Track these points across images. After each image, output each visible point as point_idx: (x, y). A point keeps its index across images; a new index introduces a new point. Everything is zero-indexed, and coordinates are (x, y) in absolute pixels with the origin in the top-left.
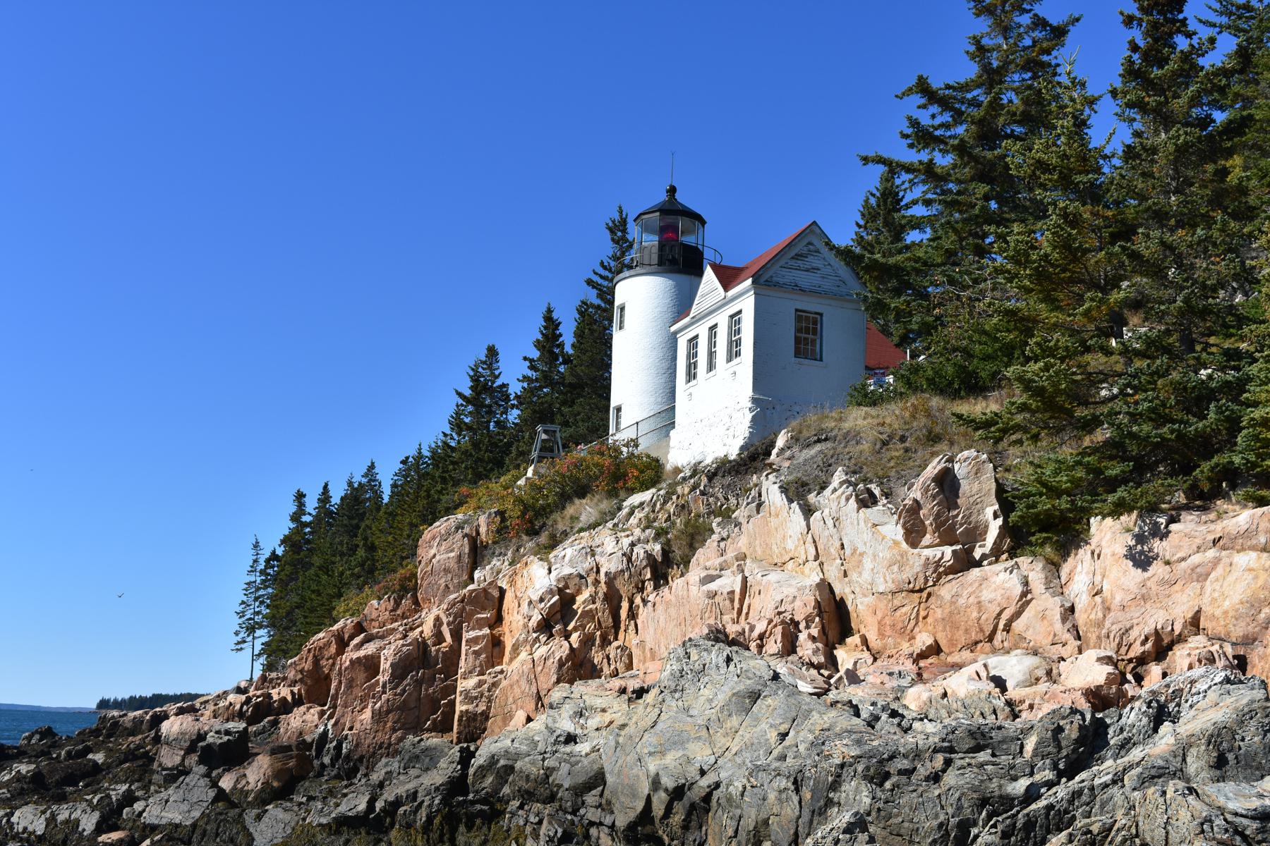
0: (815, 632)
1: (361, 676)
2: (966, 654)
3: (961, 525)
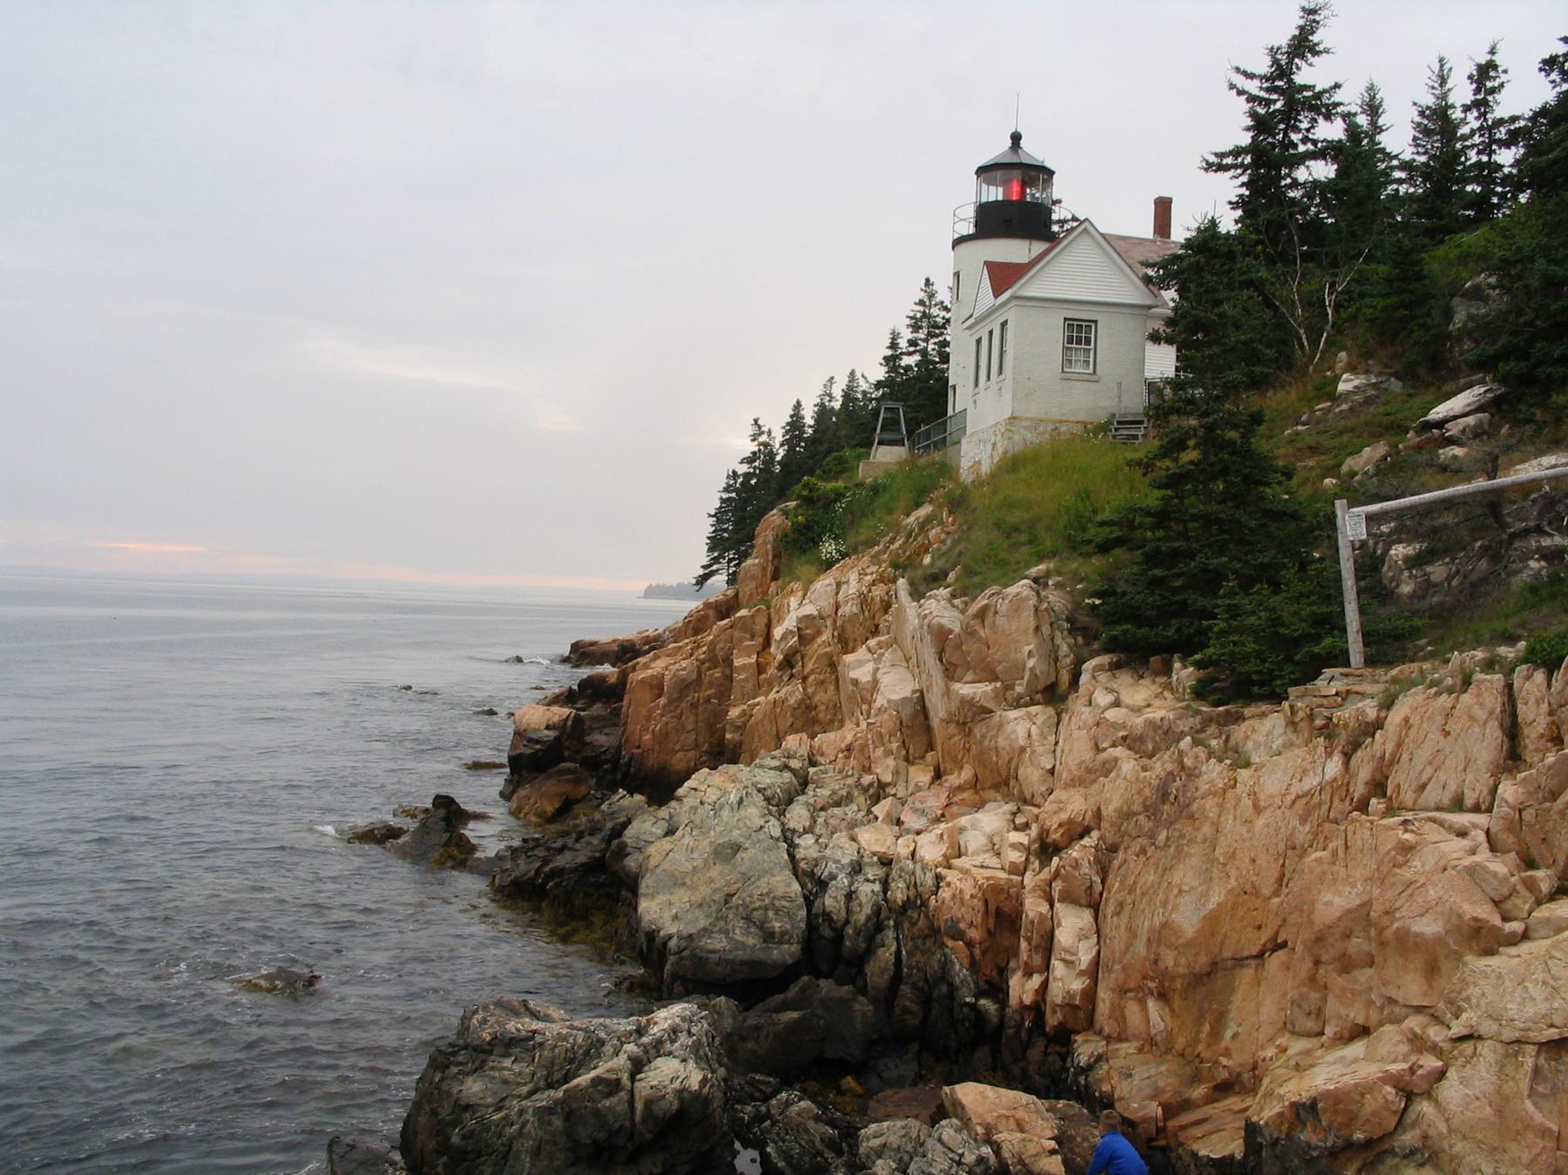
0: (895, 745)
1: (647, 695)
3: (1000, 662)
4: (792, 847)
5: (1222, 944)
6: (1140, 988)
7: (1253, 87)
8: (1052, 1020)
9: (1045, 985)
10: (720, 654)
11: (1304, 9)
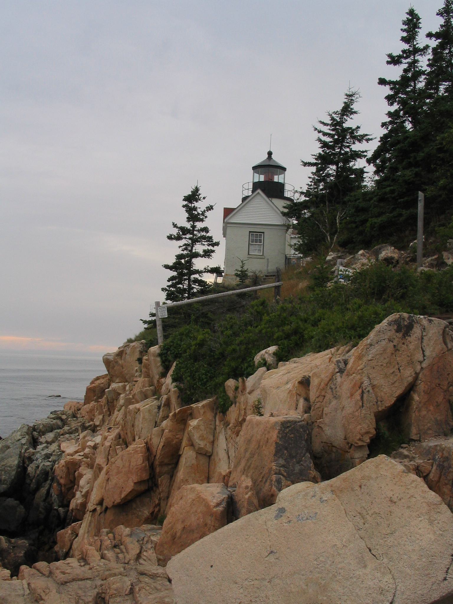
3: (127, 374)
7: (326, 129)
11: (347, 95)
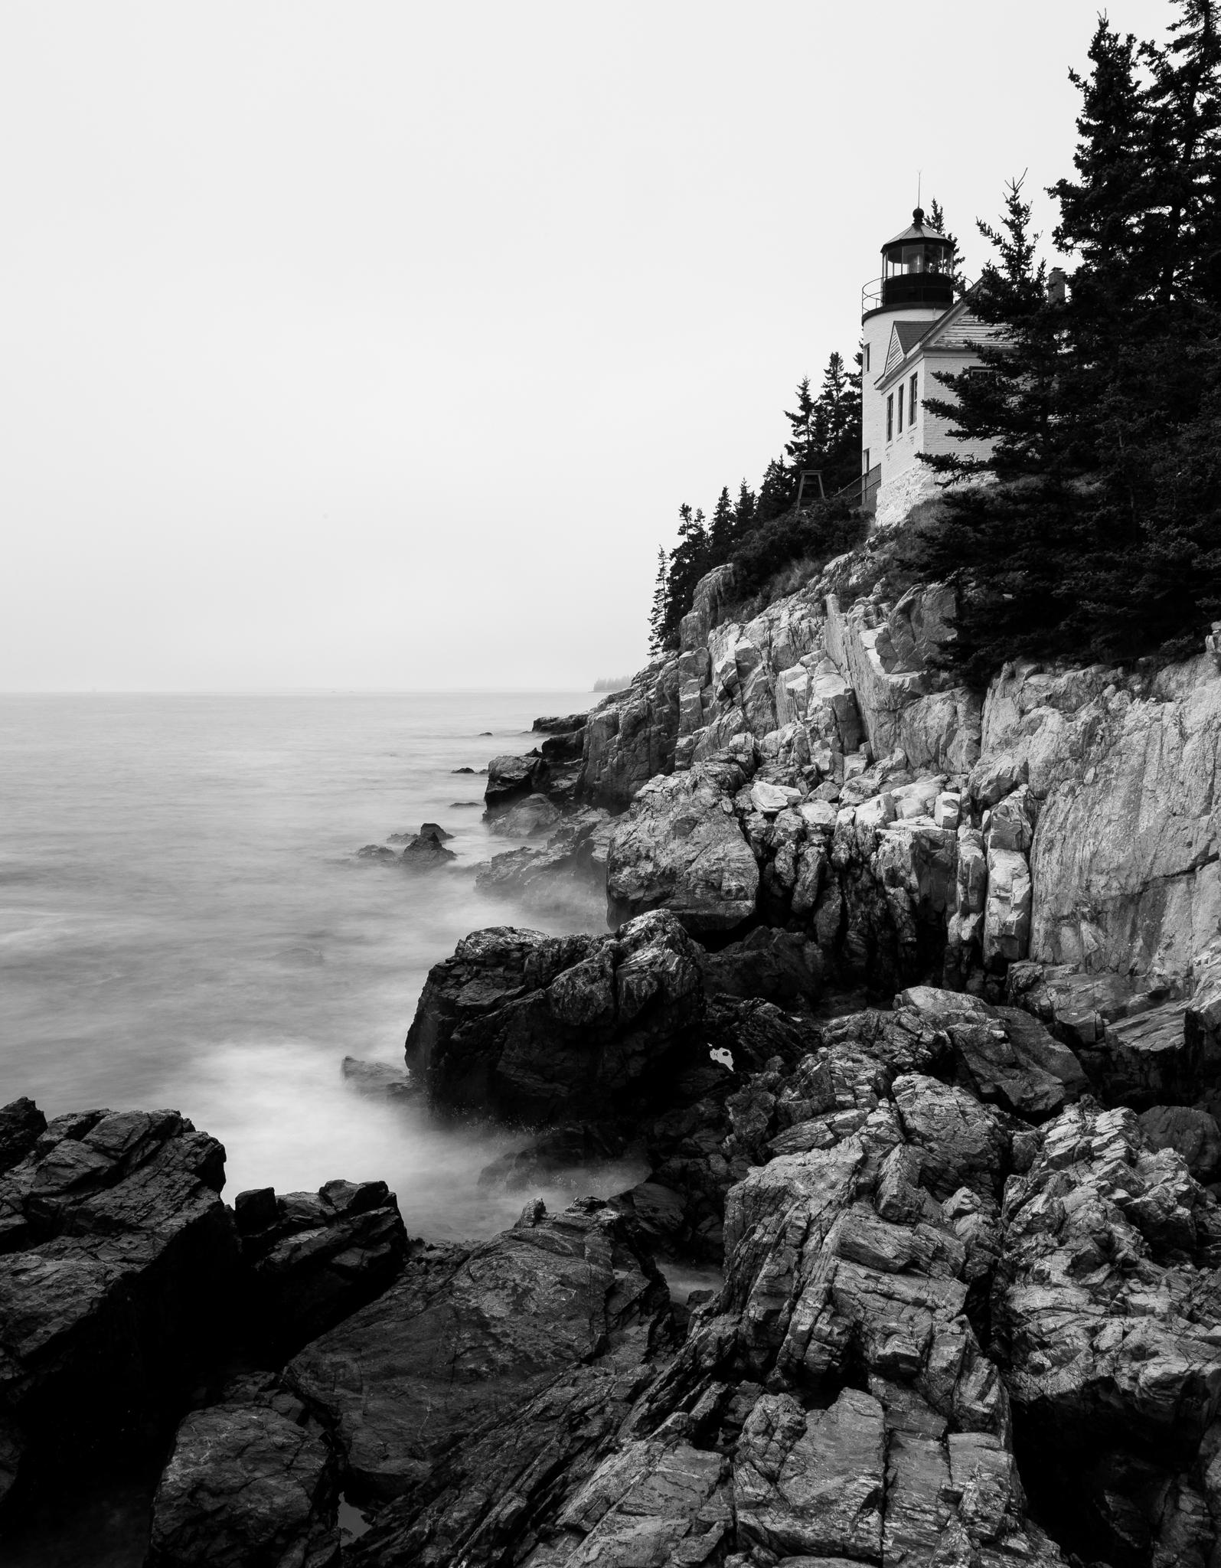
0: (830, 739)
2: (923, 771)
4: (743, 823)
5: (1152, 863)
6: (1073, 914)
8: (990, 951)
9: (980, 925)
10: (667, 692)
